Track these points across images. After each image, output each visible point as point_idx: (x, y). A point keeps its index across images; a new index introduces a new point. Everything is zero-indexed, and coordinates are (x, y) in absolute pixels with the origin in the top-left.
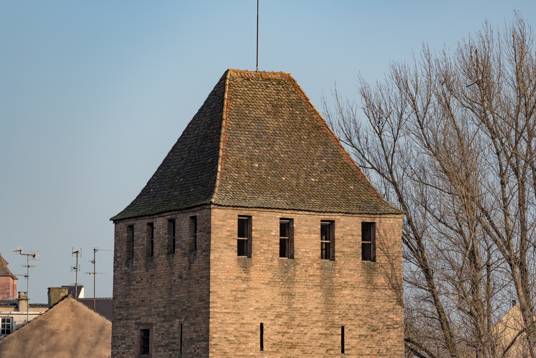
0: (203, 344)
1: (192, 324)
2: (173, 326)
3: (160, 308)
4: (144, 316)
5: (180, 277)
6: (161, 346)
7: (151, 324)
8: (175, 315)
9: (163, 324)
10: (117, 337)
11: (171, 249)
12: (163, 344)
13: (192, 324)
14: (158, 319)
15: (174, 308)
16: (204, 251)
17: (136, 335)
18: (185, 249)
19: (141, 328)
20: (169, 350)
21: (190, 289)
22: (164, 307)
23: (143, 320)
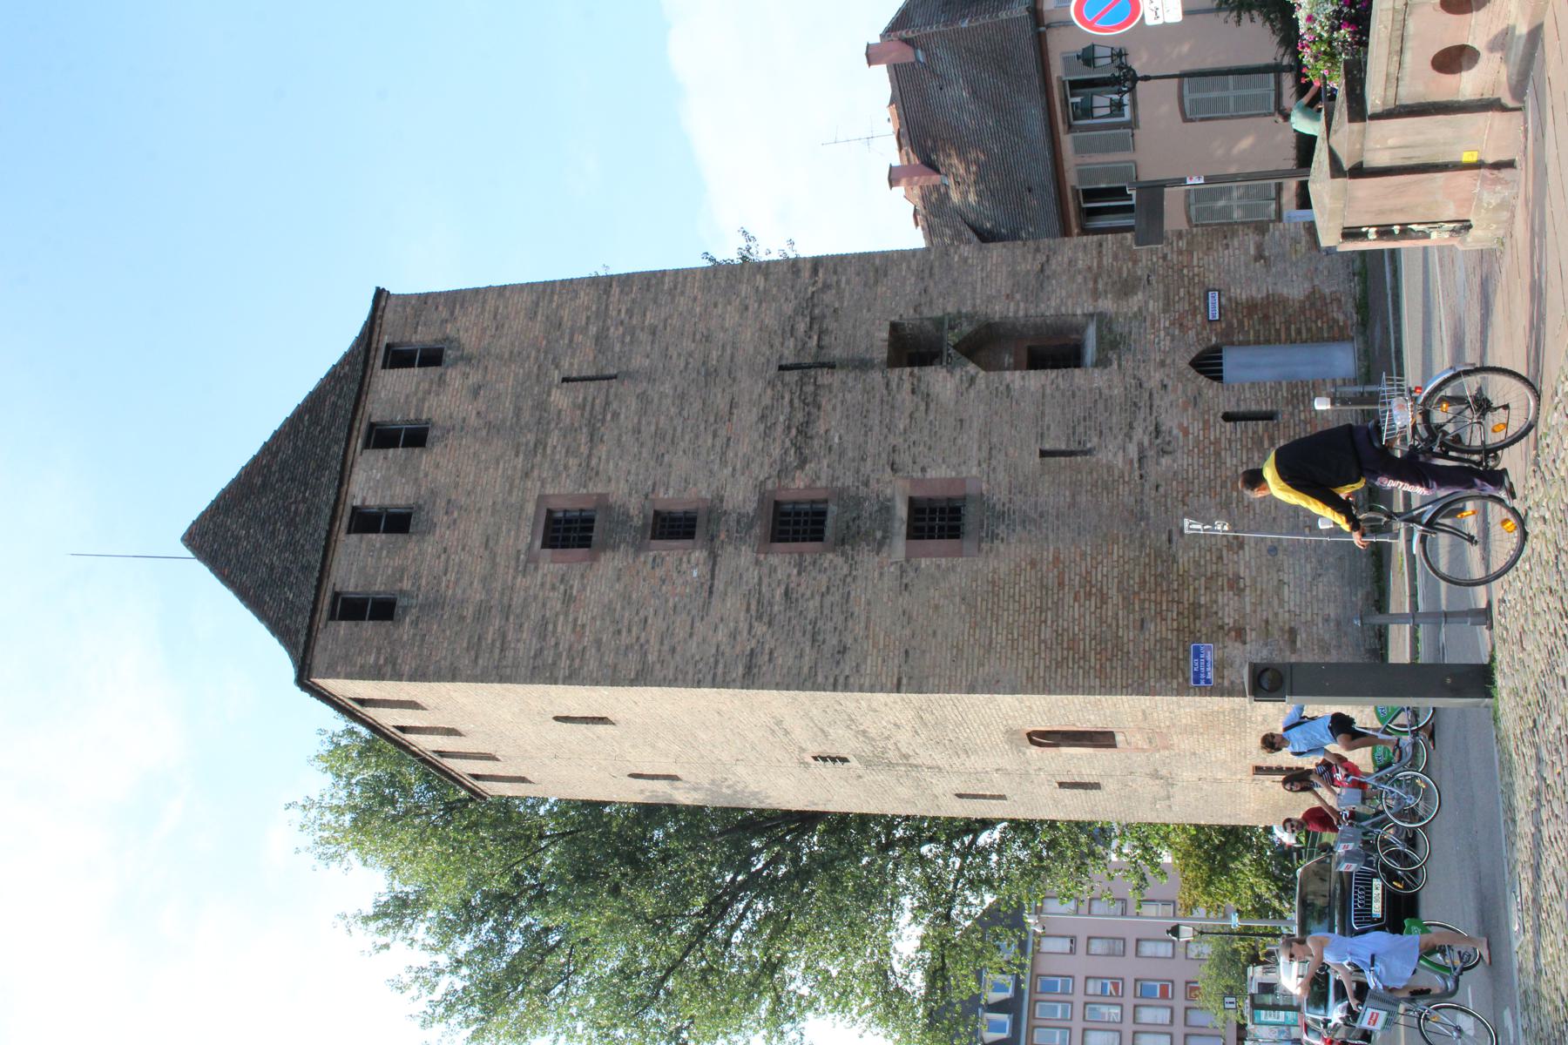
0: (615, 290)
1: (571, 341)
2: (560, 411)
3: (515, 467)
4: (517, 537)
5: (476, 391)
6: (589, 456)
7: (542, 498)
8: (541, 406)
9: (549, 451)
10: (535, 657)
11: (417, 437)
12: (586, 452)
13: (571, 341)
14: (536, 473)
15: (526, 416)
16: (452, 313)
17: (552, 565)
18: (431, 382)
19: (538, 543)
20: (603, 421)
21: (506, 356)
22: (517, 455)
23: (526, 531)
